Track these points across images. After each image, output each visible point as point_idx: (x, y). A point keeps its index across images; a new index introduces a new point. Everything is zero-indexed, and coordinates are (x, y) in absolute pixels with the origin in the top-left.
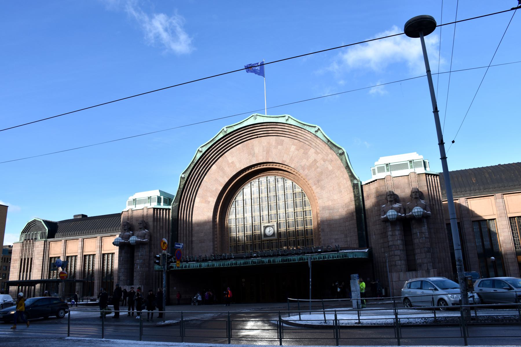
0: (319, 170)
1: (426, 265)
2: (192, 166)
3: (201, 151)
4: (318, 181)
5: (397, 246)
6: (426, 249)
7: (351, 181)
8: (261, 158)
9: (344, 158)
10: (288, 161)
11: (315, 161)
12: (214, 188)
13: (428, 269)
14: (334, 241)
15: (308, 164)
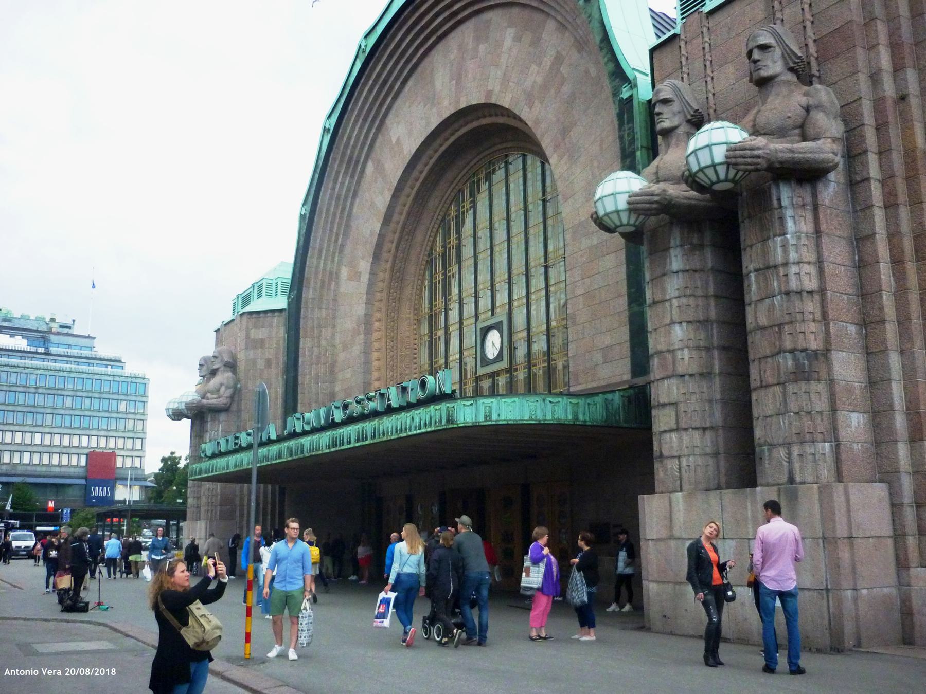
0: (566, 89)
1: (782, 453)
2: (317, 176)
3: (329, 130)
4: (565, 132)
5: (669, 356)
6: (788, 362)
7: (616, 93)
8: (446, 103)
9: (595, 7)
10: (497, 89)
11: (558, 59)
12: (369, 232)
13: (791, 480)
14: (598, 357)
15: (539, 80)
